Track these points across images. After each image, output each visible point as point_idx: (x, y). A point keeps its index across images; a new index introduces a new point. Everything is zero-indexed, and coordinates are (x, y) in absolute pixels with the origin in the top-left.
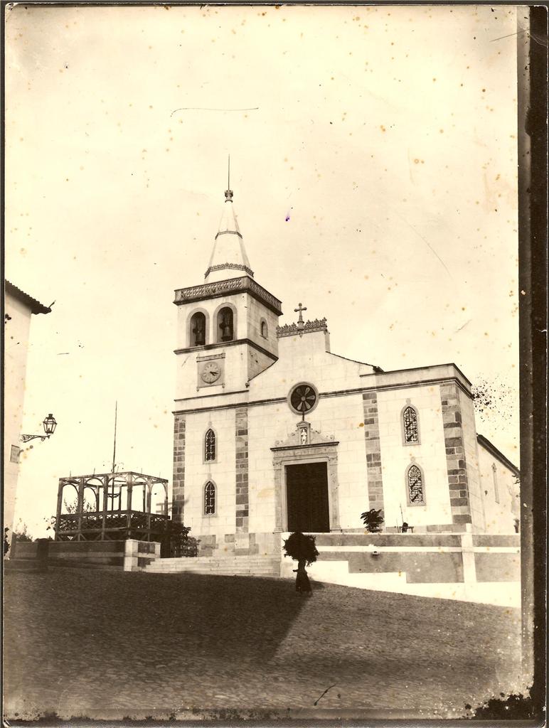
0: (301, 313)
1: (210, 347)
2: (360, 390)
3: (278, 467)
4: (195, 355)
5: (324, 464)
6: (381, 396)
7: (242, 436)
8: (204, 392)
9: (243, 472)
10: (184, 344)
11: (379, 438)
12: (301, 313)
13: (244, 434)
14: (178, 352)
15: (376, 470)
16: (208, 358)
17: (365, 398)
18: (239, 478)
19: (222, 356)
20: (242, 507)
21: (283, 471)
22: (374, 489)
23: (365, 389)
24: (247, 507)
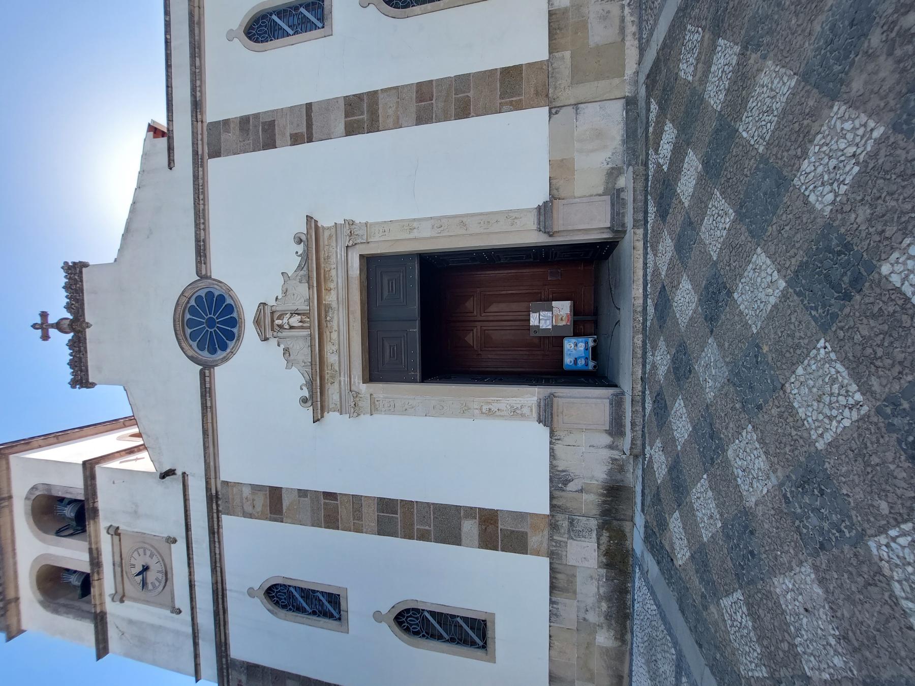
0: (52, 326)
1: (96, 561)
2: (198, 162)
3: (365, 404)
4: (112, 608)
5: (370, 263)
6: (212, 114)
7: (286, 503)
8: (182, 600)
9: (370, 514)
10: (87, 629)
11: (309, 106)
12: (52, 326)
13: (280, 499)
14: (102, 649)
15: (387, 107)
16: (118, 569)
17: (216, 153)
18: (385, 529)
19: (115, 532)
20: (470, 527)
21: (380, 390)
22: (438, 105)
23: (195, 144)
24: (470, 512)
